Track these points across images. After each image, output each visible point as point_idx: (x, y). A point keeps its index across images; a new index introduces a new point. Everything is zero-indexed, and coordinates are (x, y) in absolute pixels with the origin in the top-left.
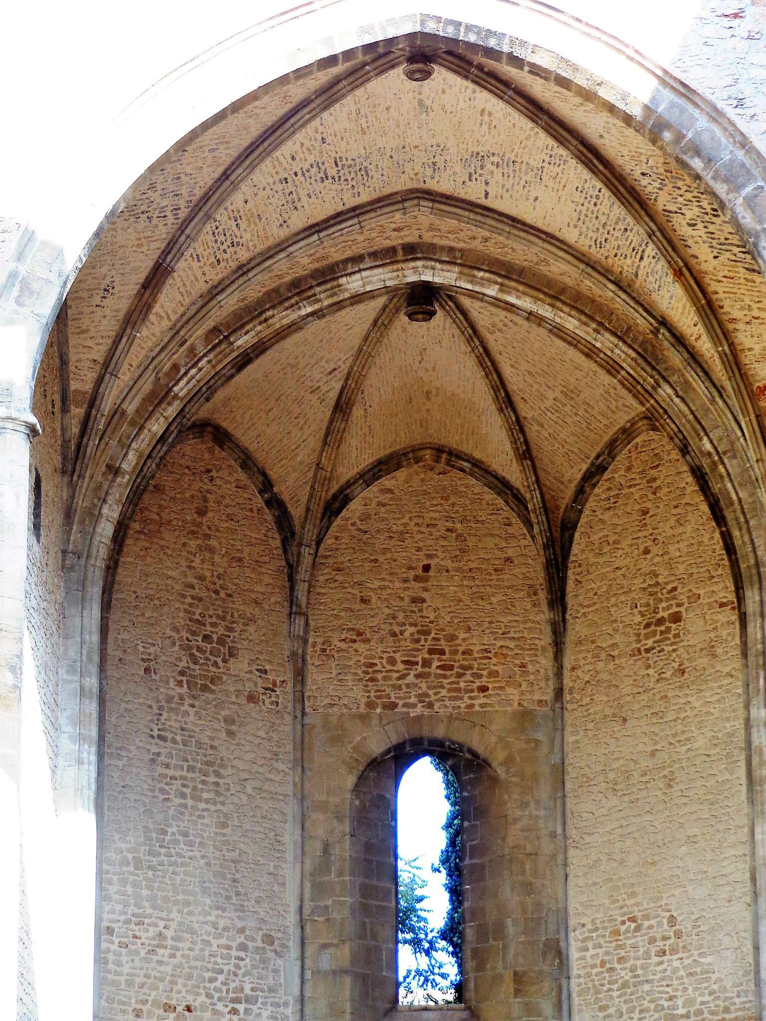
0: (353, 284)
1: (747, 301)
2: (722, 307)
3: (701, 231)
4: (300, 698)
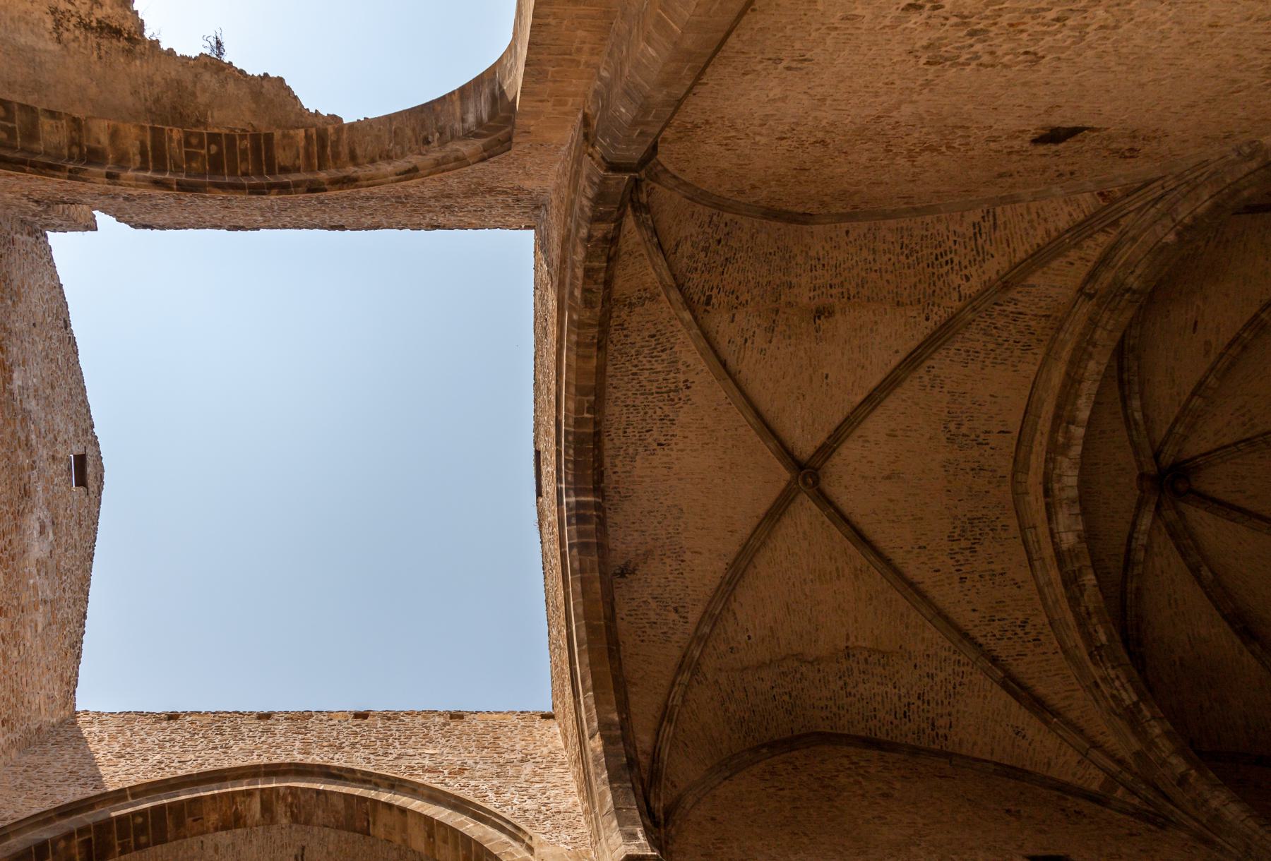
0: (1068, 539)
1: (1026, 225)
2: (1038, 245)
3: (972, 270)
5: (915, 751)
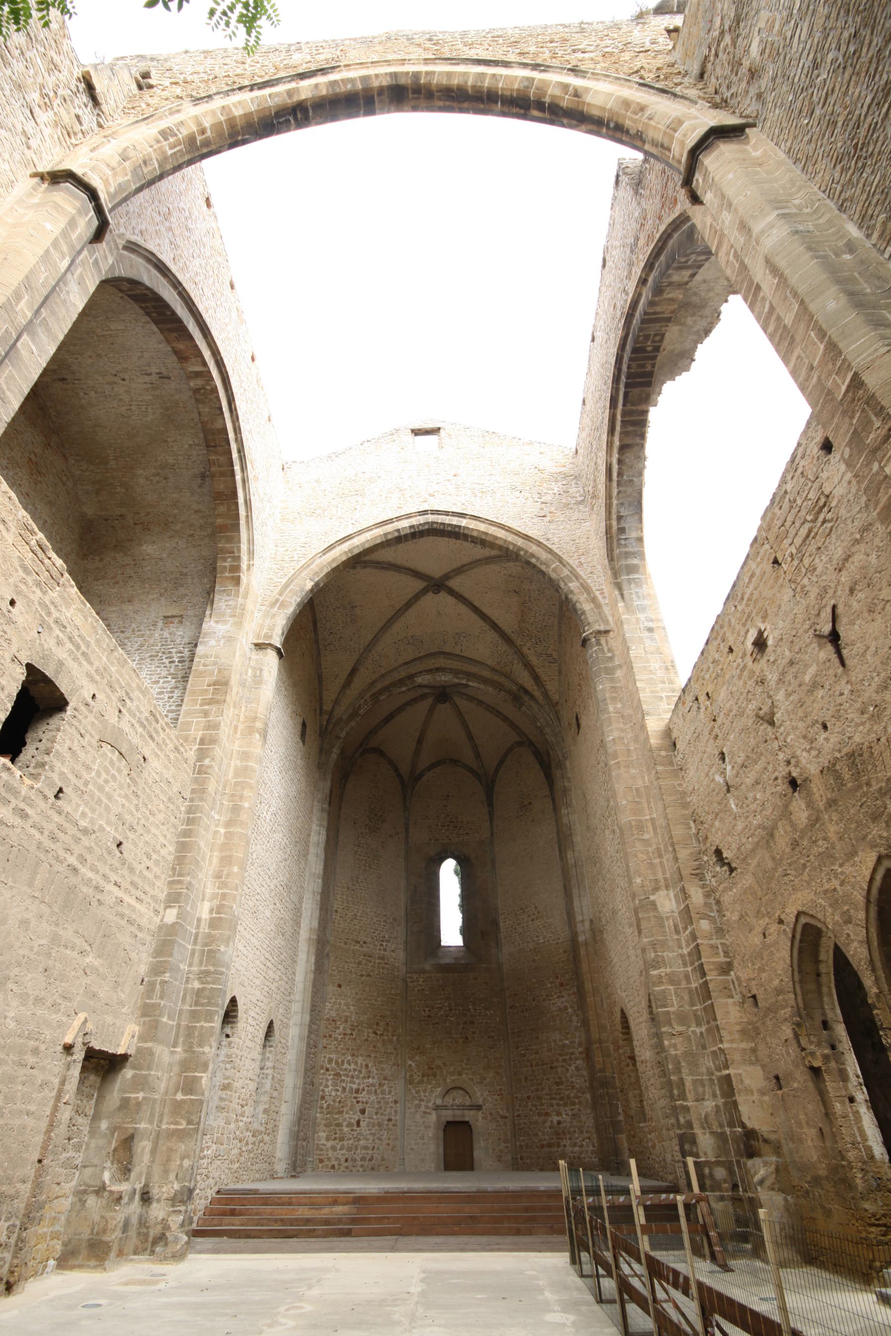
0: (419, 680)
4: (407, 838)
5: (317, 642)
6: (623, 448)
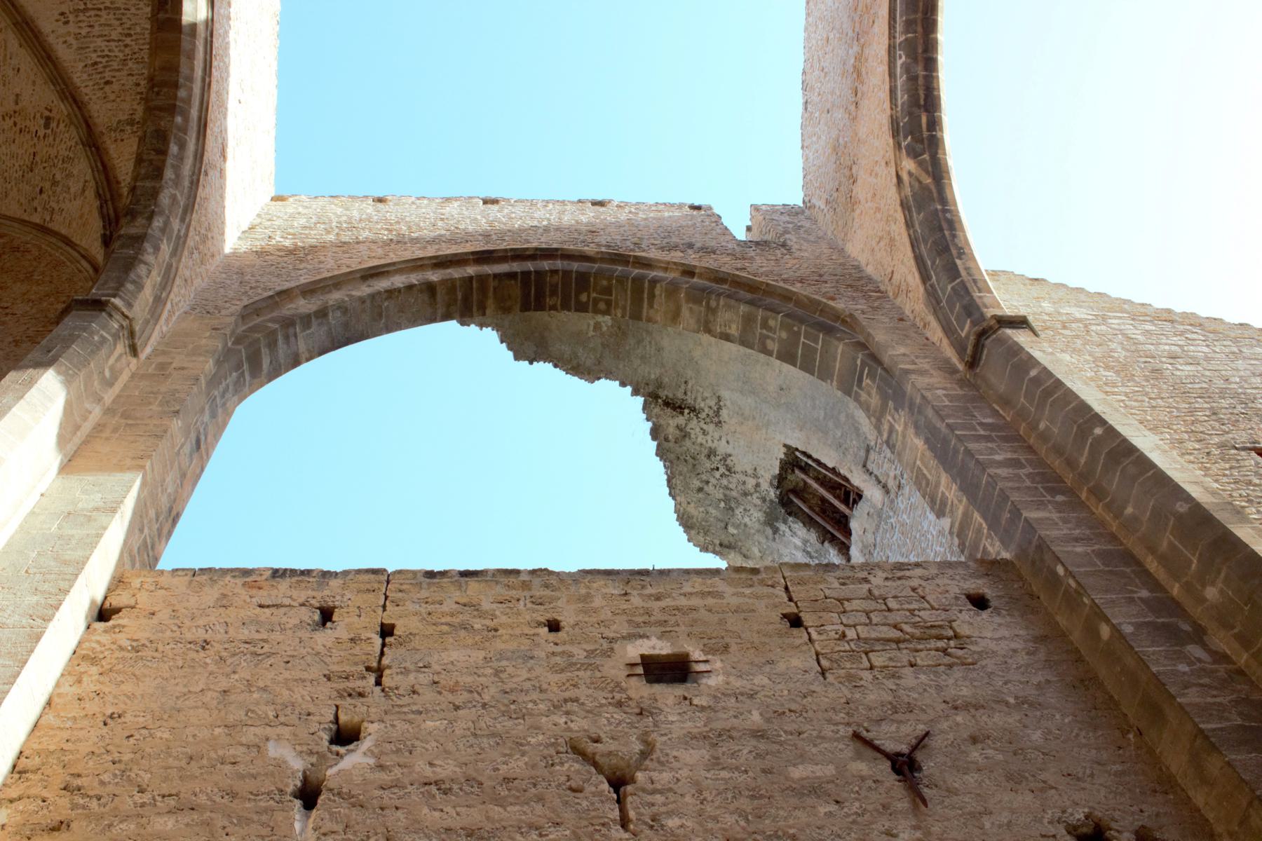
6: (430, 289)
